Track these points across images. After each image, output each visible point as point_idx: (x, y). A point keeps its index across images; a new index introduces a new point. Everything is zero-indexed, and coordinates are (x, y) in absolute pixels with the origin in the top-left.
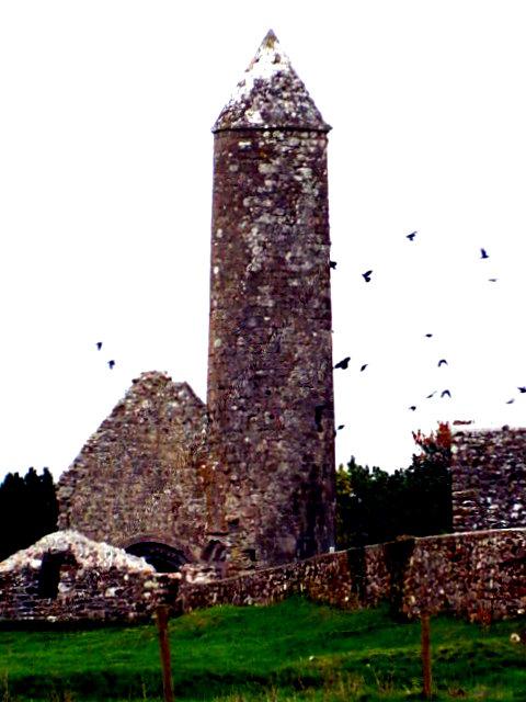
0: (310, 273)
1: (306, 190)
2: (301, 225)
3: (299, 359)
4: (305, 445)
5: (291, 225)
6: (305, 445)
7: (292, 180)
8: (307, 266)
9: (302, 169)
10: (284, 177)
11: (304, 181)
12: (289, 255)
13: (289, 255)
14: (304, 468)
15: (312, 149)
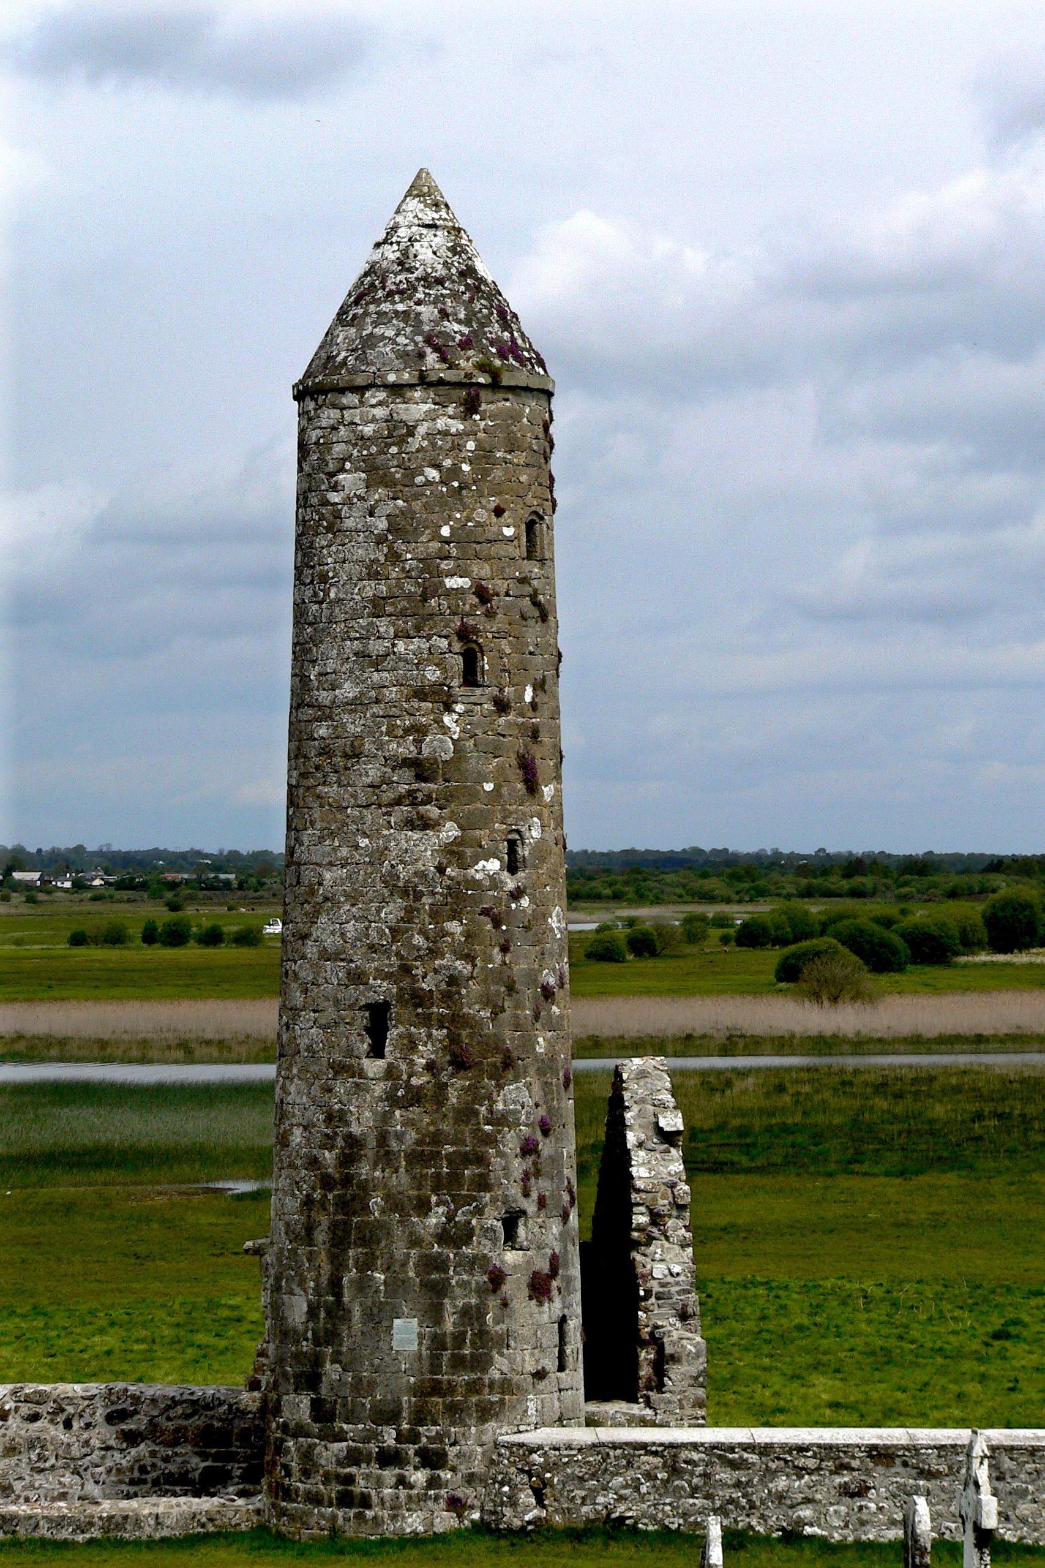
0: (356, 704)
1: (349, 523)
2: (339, 601)
3: (326, 899)
4: (330, 1090)
5: (320, 603)
6: (330, 1090)
7: (326, 503)
8: (348, 690)
11: (348, 502)
14: (328, 1142)
15: (368, 430)
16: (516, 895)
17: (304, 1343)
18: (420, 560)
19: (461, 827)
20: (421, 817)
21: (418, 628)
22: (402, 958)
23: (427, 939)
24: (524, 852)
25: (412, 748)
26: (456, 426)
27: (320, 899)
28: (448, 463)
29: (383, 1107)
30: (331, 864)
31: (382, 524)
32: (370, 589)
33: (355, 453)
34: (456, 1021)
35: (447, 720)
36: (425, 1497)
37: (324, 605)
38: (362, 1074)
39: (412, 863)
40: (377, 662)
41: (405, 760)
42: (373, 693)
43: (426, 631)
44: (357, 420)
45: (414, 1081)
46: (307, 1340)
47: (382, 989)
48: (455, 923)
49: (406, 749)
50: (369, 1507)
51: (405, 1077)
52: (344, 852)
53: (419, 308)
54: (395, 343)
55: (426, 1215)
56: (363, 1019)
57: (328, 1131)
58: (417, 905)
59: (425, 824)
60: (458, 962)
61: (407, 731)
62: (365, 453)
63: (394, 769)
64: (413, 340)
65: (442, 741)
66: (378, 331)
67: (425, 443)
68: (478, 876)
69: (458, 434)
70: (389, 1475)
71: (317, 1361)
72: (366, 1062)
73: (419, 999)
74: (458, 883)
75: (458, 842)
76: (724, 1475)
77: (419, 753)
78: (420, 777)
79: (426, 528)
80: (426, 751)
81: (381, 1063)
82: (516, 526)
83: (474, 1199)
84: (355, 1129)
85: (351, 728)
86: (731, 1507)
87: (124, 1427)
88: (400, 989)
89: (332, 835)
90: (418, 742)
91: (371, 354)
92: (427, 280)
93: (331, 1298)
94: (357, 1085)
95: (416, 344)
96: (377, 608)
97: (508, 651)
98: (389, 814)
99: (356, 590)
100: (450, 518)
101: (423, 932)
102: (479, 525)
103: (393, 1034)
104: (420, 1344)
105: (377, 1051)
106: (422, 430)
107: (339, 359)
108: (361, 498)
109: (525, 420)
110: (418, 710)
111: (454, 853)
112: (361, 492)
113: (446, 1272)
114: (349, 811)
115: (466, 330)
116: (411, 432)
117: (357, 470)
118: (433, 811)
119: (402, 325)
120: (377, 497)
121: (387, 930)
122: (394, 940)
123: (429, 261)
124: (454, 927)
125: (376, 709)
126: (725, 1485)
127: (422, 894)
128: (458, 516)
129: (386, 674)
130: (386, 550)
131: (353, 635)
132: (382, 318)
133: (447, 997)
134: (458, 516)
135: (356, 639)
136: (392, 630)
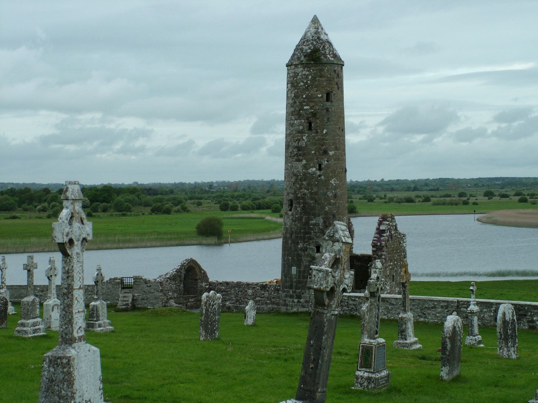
16: (320, 176)
18: (299, 103)
20: (299, 159)
22: (295, 190)
24: (323, 166)
28: (305, 81)
31: (293, 95)
34: (305, 203)
36: (297, 305)
39: (297, 169)
42: (291, 132)
45: (296, 216)
49: (295, 144)
50: (288, 306)
54: (297, 55)
59: (299, 160)
67: (301, 77)
68: (310, 172)
69: (308, 75)
70: (291, 300)
72: (289, 212)
73: (297, 198)
75: (305, 164)
76: (351, 302)
81: (291, 212)
86: (353, 310)
90: (298, 143)
97: (319, 122)
98: (293, 158)
100: (305, 93)
101: (298, 184)
102: (311, 94)
104: (296, 272)
106: (300, 74)
109: (326, 71)
111: (305, 167)
112: (290, 88)
116: (298, 75)
118: (301, 158)
124: (304, 183)
126: (351, 305)
127: (298, 176)
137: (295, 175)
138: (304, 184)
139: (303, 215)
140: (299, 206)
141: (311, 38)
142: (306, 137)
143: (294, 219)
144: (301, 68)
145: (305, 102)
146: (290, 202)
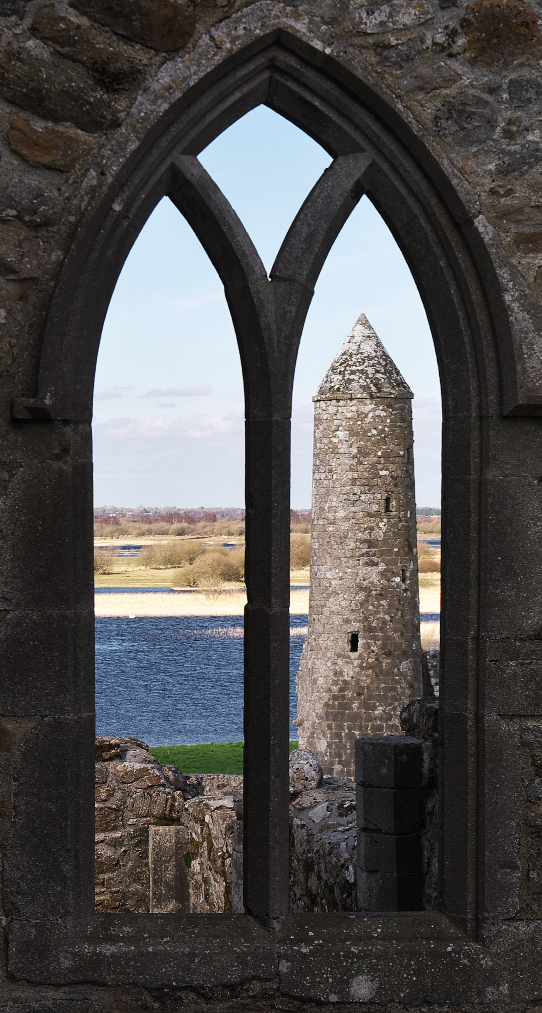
0: (345, 519)
1: (341, 451)
3: (333, 592)
4: (336, 664)
5: (329, 480)
7: (331, 442)
8: (341, 514)
9: (338, 433)
10: (325, 441)
11: (340, 442)
12: (327, 505)
13: (327, 505)
15: (349, 415)
17: (326, 757)
18: (370, 465)
19: (386, 565)
20: (371, 561)
21: (370, 490)
23: (374, 607)
25: (368, 536)
26: (383, 414)
27: (331, 592)
28: (380, 427)
29: (357, 670)
30: (335, 579)
31: (355, 451)
32: (350, 475)
33: (344, 424)
35: (381, 525)
37: (331, 481)
38: (349, 657)
40: (353, 503)
41: (365, 540)
43: (373, 491)
44: (344, 411)
45: (370, 660)
46: (327, 756)
47: (355, 626)
48: (384, 601)
49: (366, 536)
51: (366, 659)
52: (341, 574)
53: (367, 369)
54: (358, 382)
55: (375, 710)
56: (348, 637)
57: (335, 679)
58: (370, 594)
60: (386, 616)
61: (366, 529)
62: (348, 424)
63: (361, 543)
64: (365, 381)
65: (378, 532)
66: (352, 377)
67: (371, 420)
71: (332, 763)
72: (351, 654)
73: (369, 629)
74: (386, 586)
75: (385, 570)
77: (370, 537)
78: (369, 547)
79: (372, 452)
80: (373, 537)
82: (404, 451)
83: (392, 704)
84: (346, 678)
85: (342, 528)
87: (223, 790)
88: (364, 626)
89: (335, 567)
91: (350, 386)
92: (370, 358)
93: (337, 741)
94: (347, 662)
95: (367, 382)
96: (354, 482)
98: (359, 560)
99: (345, 476)
100: (381, 448)
101: (372, 604)
102: (391, 451)
103: (361, 643)
105: (354, 648)
106: (370, 415)
107: (336, 388)
108: (346, 441)
110: (370, 521)
111: (383, 574)
112: (347, 439)
113: (382, 730)
114: (342, 559)
115: (385, 377)
116: (366, 416)
117: (345, 430)
118: (375, 559)
119: (361, 375)
120: (353, 440)
121: (359, 604)
122: (362, 608)
123: (368, 350)
124: (383, 602)
125: (354, 521)
128: (384, 447)
129: (356, 507)
130: (357, 461)
131: (343, 492)
132: (353, 373)
133: (382, 629)
134: (384, 447)
135: (345, 494)
136: (359, 491)
137: (365, 589)
138: (383, 605)
139: (384, 658)
140: (375, 643)
141: (374, 354)
142: (384, 524)
143: (364, 665)
144: (371, 404)
145: (380, 463)
146: (350, 635)
